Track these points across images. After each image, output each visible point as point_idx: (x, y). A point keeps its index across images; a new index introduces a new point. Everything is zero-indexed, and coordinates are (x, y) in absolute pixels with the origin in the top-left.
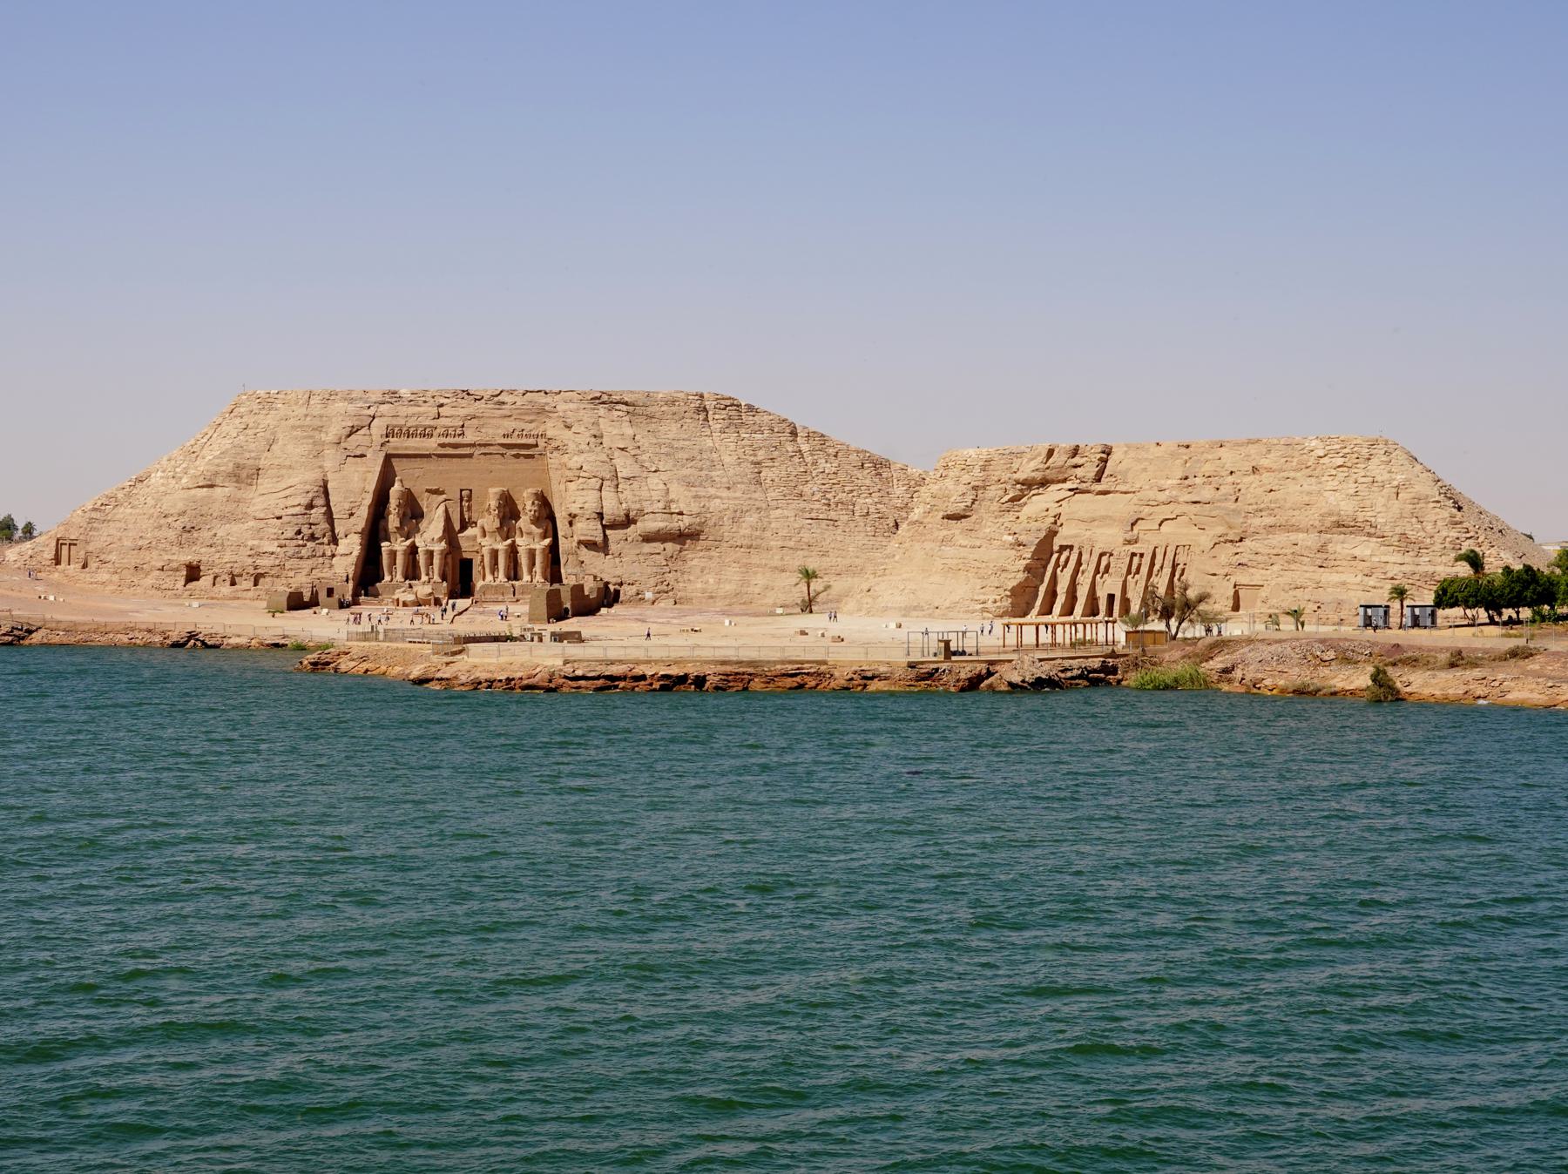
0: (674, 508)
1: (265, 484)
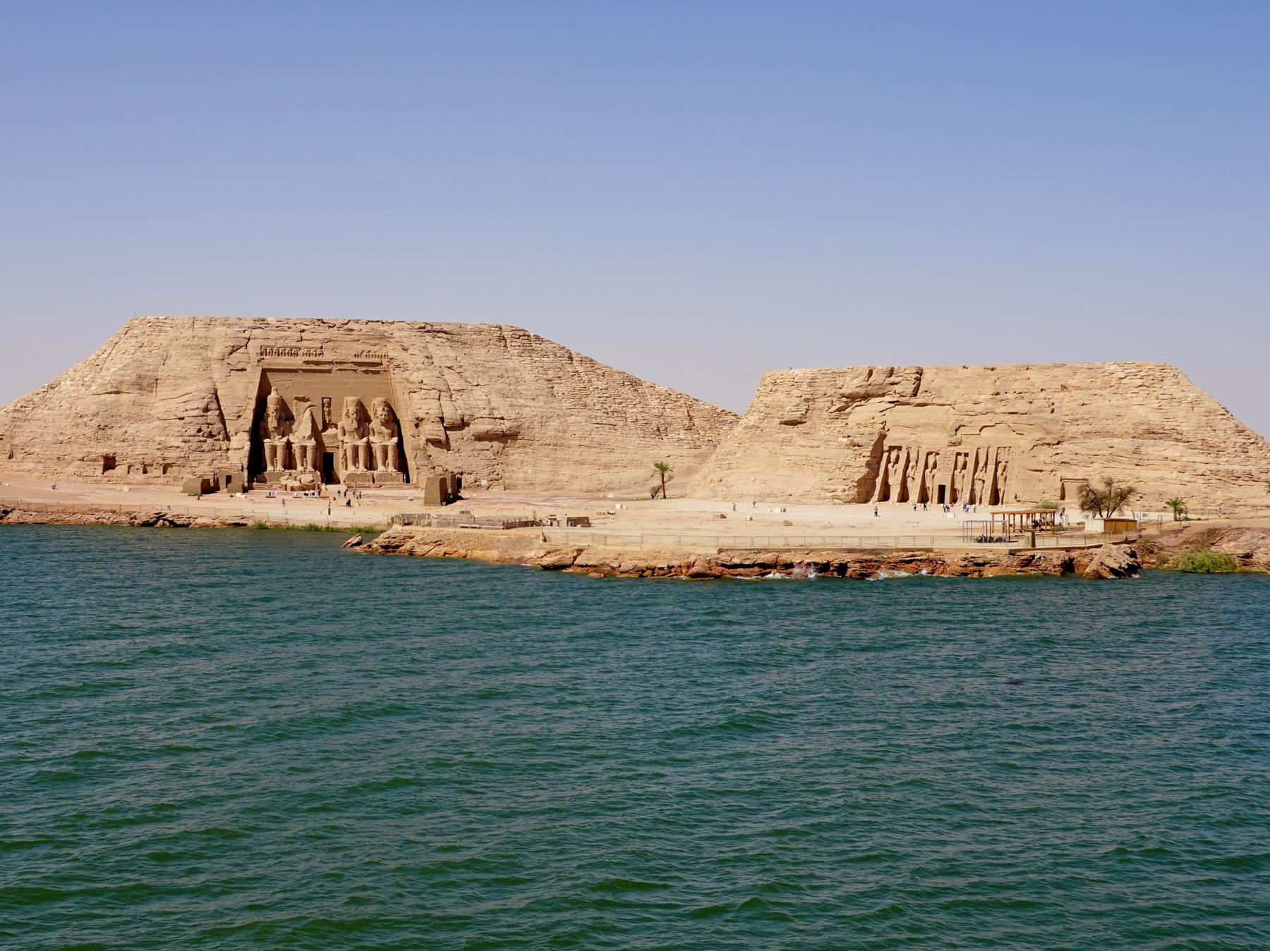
0: (496, 414)
1: (163, 391)
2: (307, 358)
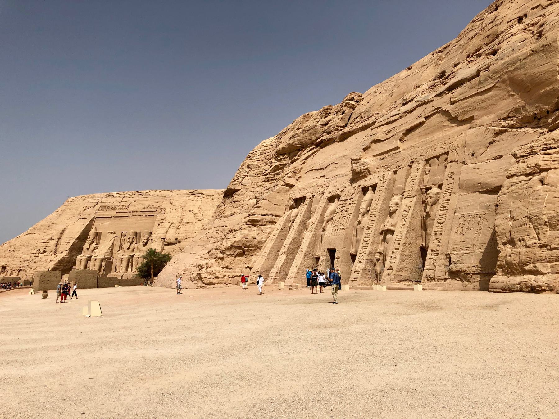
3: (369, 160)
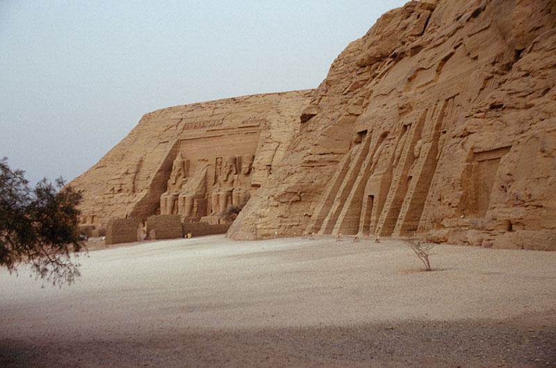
2: (211, 128)
3: (412, 94)
